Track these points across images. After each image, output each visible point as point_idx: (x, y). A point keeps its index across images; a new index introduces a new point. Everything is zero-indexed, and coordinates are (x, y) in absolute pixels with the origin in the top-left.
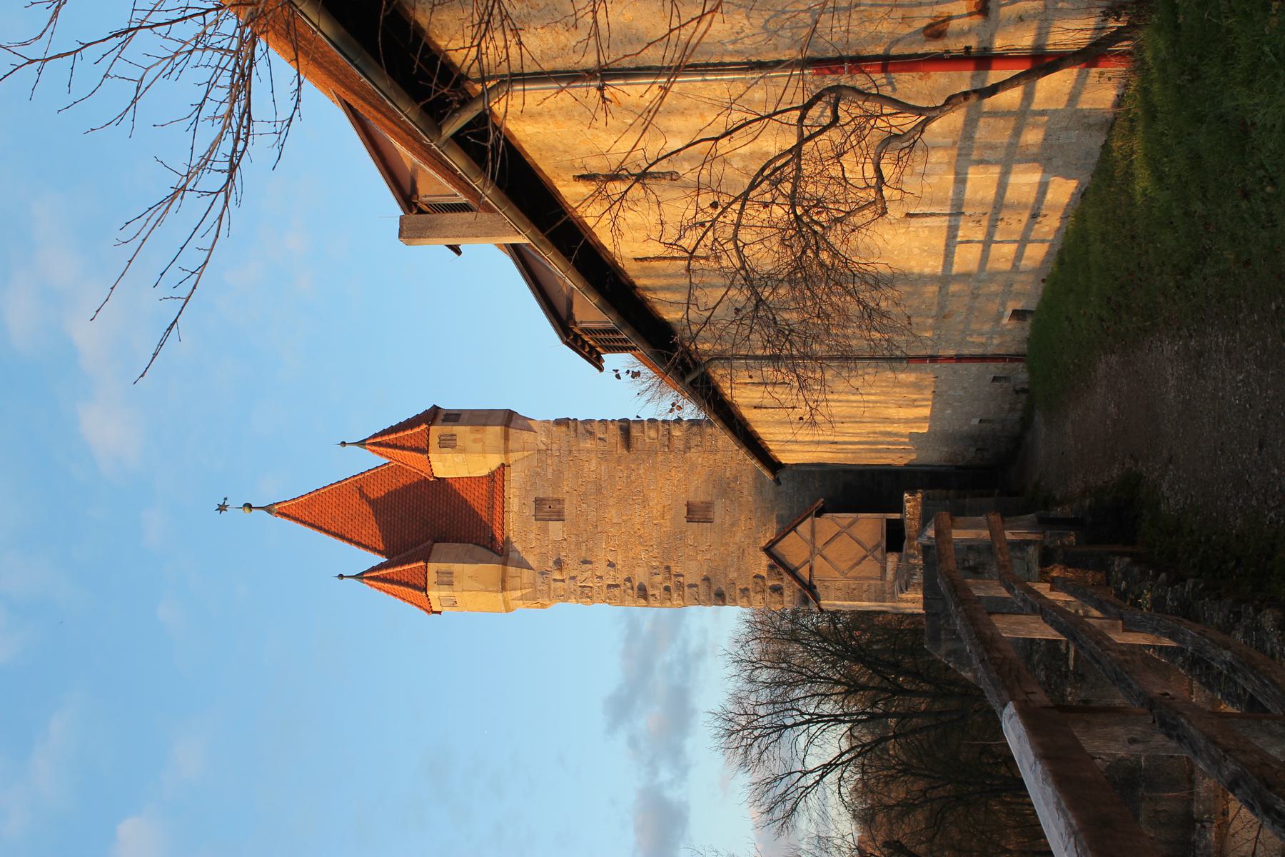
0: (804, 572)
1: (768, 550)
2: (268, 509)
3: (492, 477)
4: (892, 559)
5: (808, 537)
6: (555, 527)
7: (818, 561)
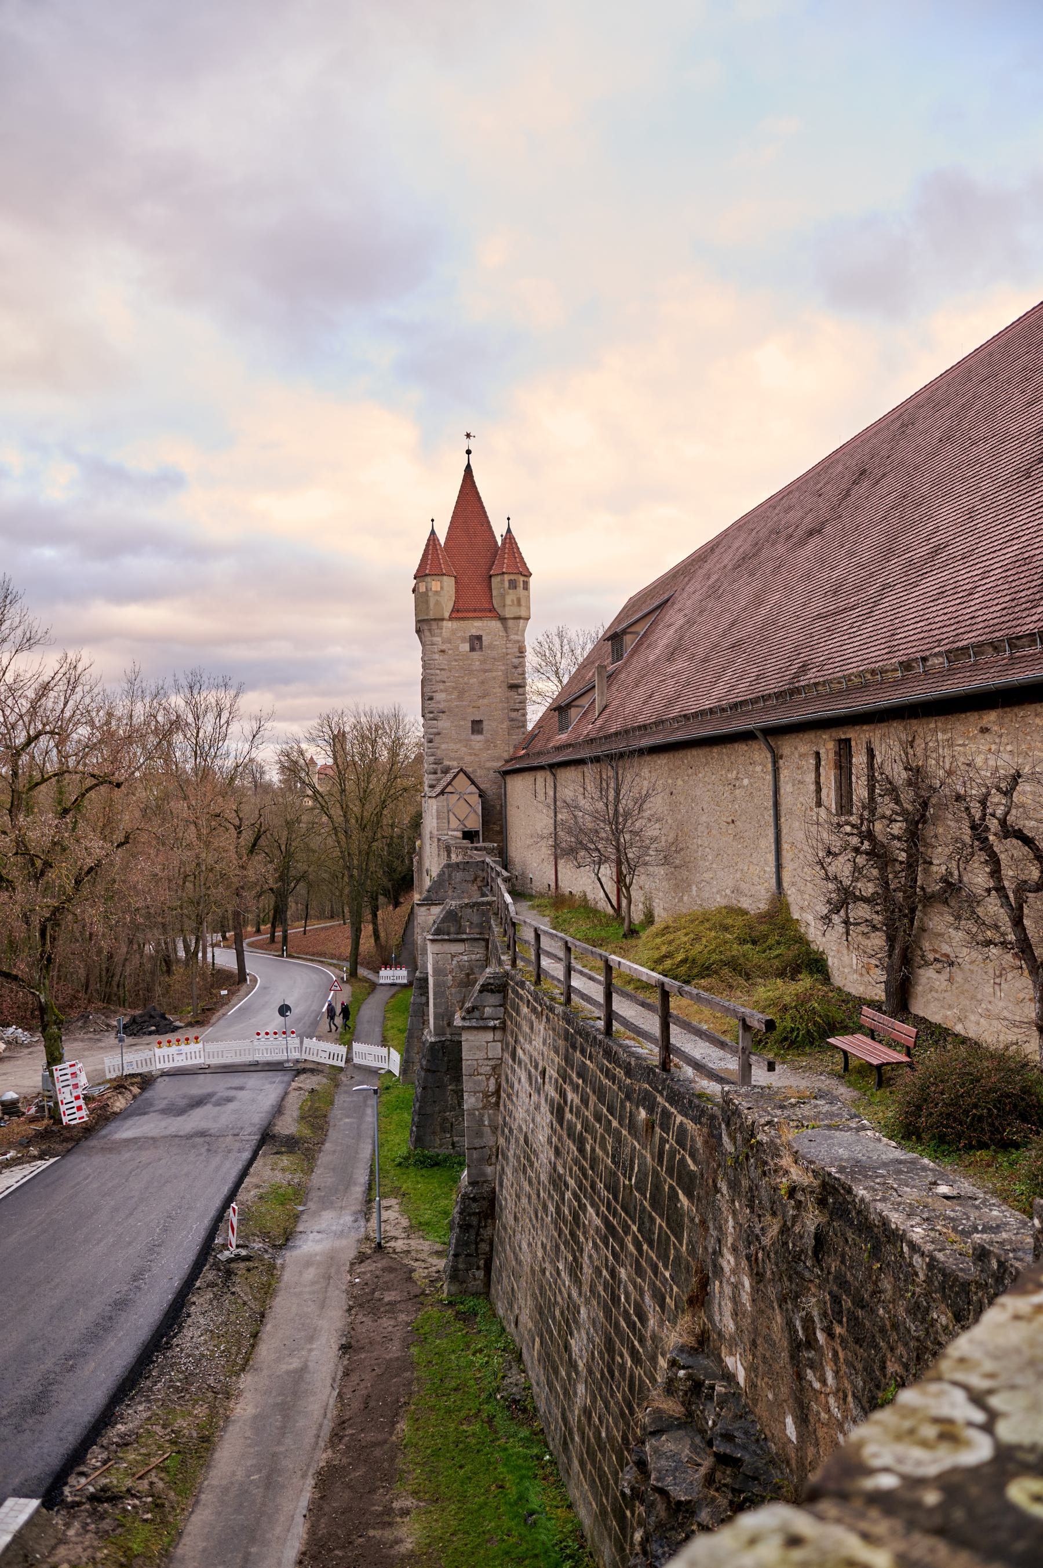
0: (449, 789)
1: (461, 770)
2: (468, 467)
3: (492, 610)
4: (459, 834)
5: (468, 791)
6: (466, 647)
7: (456, 797)
